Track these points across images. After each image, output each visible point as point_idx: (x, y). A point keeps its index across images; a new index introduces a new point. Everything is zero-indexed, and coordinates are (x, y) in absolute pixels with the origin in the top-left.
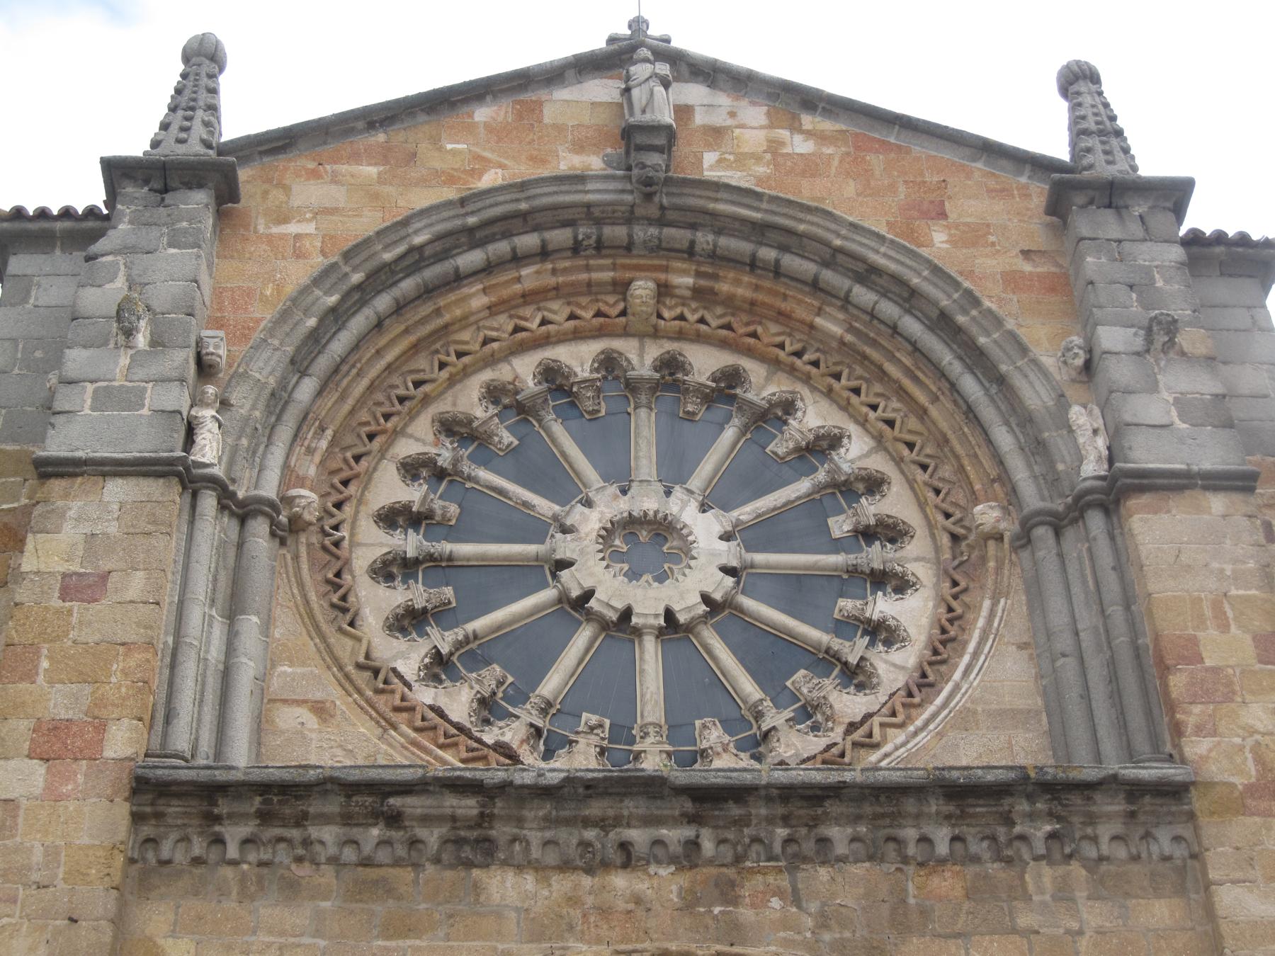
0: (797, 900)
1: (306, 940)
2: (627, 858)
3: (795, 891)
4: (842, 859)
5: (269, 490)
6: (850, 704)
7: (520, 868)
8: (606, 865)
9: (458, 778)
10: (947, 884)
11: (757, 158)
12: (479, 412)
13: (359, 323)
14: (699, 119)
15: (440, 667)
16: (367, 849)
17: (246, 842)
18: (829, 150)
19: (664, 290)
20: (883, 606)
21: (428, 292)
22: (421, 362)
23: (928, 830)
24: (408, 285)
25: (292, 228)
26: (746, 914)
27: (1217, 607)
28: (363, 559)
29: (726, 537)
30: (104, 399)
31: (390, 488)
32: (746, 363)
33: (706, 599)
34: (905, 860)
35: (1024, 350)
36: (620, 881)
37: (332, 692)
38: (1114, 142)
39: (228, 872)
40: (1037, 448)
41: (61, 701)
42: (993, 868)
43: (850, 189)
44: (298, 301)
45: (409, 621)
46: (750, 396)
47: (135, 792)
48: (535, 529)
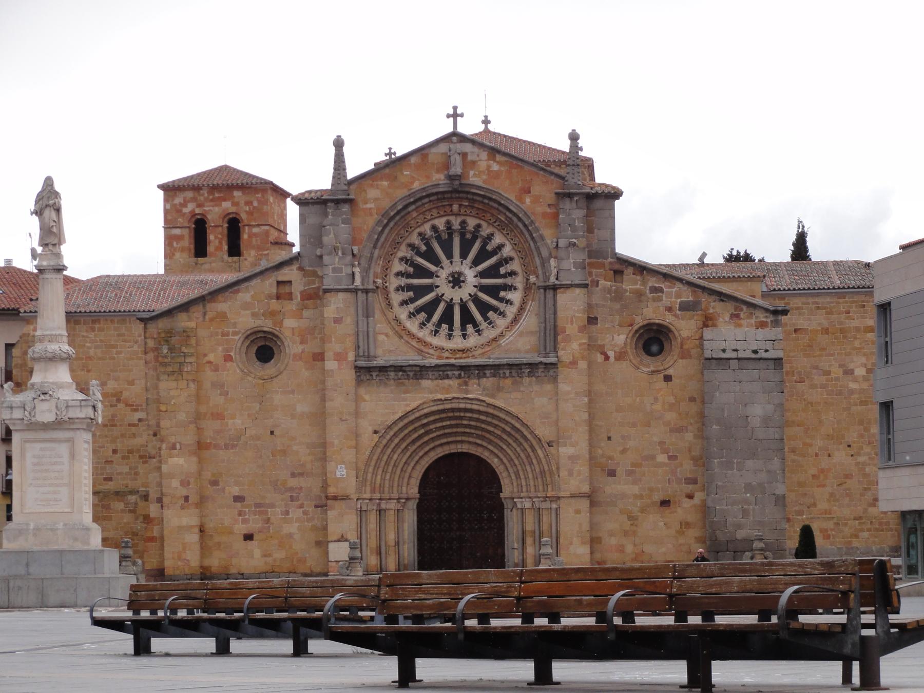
0: (479, 385)
2: (447, 377)
5: (371, 286)
6: (501, 323)
8: (444, 379)
10: (508, 382)
11: (483, 172)
13: (386, 231)
14: (470, 158)
15: (411, 315)
18: (502, 169)
19: (460, 206)
20: (510, 295)
21: (402, 217)
22: (402, 232)
24: (397, 218)
26: (470, 388)
27: (572, 319)
28: (392, 288)
29: (475, 276)
30: (334, 270)
31: (398, 267)
32: (482, 223)
33: (470, 295)
35: (542, 238)
36: (446, 381)
37: (391, 333)
40: (543, 265)
42: (518, 379)
43: (507, 183)
44: (373, 231)
45: (404, 303)
46: (482, 233)
48: (430, 275)
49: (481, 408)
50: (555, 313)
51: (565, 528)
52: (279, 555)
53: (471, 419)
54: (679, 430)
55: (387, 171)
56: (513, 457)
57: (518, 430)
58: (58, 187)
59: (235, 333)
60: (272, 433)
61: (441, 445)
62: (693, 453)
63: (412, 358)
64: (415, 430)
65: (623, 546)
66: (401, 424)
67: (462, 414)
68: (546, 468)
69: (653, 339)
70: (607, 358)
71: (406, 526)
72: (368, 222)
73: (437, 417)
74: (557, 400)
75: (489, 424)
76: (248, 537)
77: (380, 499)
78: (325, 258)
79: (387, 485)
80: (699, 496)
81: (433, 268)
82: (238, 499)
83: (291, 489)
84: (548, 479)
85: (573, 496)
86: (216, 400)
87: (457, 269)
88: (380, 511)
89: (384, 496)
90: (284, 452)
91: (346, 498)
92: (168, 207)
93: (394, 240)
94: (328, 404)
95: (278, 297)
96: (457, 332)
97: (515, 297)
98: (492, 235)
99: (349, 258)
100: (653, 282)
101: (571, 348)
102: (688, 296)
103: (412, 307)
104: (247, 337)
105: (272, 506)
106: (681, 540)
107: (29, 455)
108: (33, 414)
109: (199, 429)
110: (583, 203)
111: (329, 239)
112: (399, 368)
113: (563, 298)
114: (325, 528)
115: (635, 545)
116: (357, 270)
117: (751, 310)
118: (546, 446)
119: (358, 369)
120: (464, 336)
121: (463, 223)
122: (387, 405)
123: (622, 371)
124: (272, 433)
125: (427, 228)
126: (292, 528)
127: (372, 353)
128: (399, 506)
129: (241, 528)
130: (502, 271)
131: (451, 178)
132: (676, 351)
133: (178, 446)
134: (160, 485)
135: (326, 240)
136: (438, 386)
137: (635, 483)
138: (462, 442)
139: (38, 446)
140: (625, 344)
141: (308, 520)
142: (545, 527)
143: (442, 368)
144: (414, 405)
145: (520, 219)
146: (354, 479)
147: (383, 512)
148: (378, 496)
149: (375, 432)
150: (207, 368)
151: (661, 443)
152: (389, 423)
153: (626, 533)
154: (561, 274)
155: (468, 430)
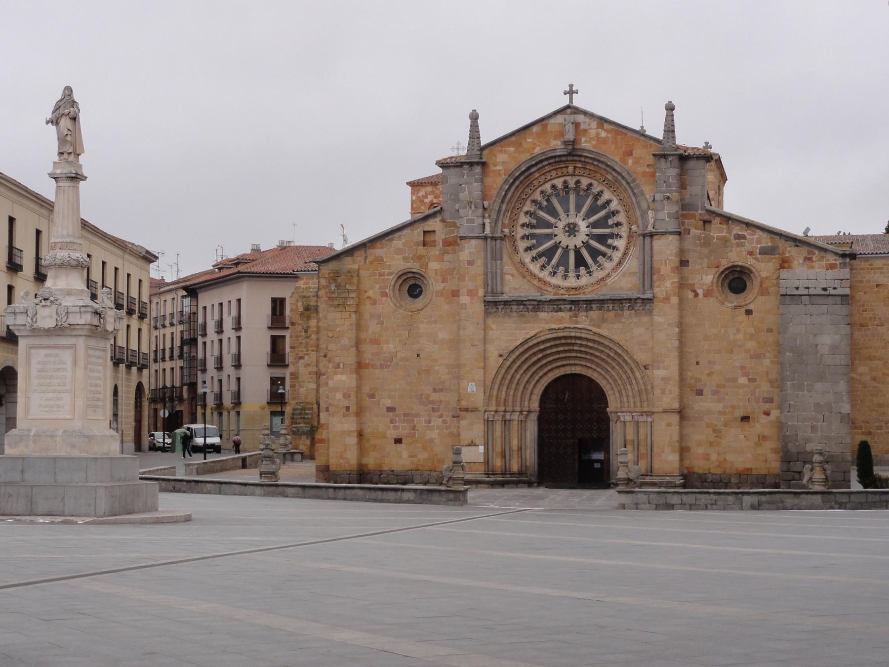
2: (560, 310)
5: (499, 235)
10: (611, 314)
12: (539, 199)
14: (582, 127)
15: (534, 259)
19: (575, 167)
24: (522, 178)
25: (498, 168)
26: (579, 319)
28: (519, 236)
30: (469, 221)
31: (523, 219)
35: (643, 194)
36: (560, 314)
37: (515, 272)
38: (671, 135)
40: (642, 216)
41: (470, 285)
42: (620, 312)
43: (613, 148)
45: (529, 249)
48: (550, 226)
49: (589, 337)
50: (652, 257)
52: (423, 456)
53: (581, 345)
54: (757, 356)
55: (513, 139)
56: (617, 378)
57: (620, 355)
58: (76, 97)
59: (390, 274)
60: (418, 355)
62: (770, 377)
63: (534, 294)
64: (535, 354)
65: (708, 455)
66: (521, 350)
67: (573, 341)
69: (736, 280)
70: (696, 295)
72: (497, 182)
73: (553, 343)
75: (596, 349)
76: (398, 441)
77: (505, 411)
78: (461, 211)
80: (775, 414)
81: (552, 220)
82: (390, 409)
83: (433, 402)
85: (665, 411)
86: (373, 328)
87: (572, 221)
88: (506, 422)
89: (508, 409)
90: (428, 372)
91: (475, 410)
92: (414, 198)
93: (519, 197)
94: (462, 332)
95: (424, 244)
96: (572, 274)
97: (621, 244)
98: (602, 192)
99: (480, 211)
100: (737, 230)
101: (666, 285)
102: (766, 241)
103: (534, 253)
104: (399, 277)
105: (418, 415)
106: (759, 451)
107: (34, 361)
108: (34, 320)
109: (359, 352)
110: (676, 162)
111: (464, 196)
112: (520, 303)
113: (659, 244)
114: (459, 435)
115: (719, 454)
116: (487, 221)
117: (823, 254)
120: (578, 277)
121: (578, 182)
123: (709, 306)
124: (418, 355)
125: (547, 187)
126: (434, 434)
127: (499, 290)
128: (522, 418)
129: (392, 434)
130: (610, 222)
131: (566, 143)
132: (756, 289)
133: (341, 365)
134: (327, 397)
135: (462, 196)
137: (719, 401)
138: (575, 365)
139: (43, 352)
140: (712, 283)
141: (447, 428)
143: (558, 303)
144: (532, 333)
145: (623, 178)
149: (501, 356)
150: (367, 302)
151: (742, 368)
152: (512, 348)
153: (711, 444)
154: (657, 224)
155: (579, 355)
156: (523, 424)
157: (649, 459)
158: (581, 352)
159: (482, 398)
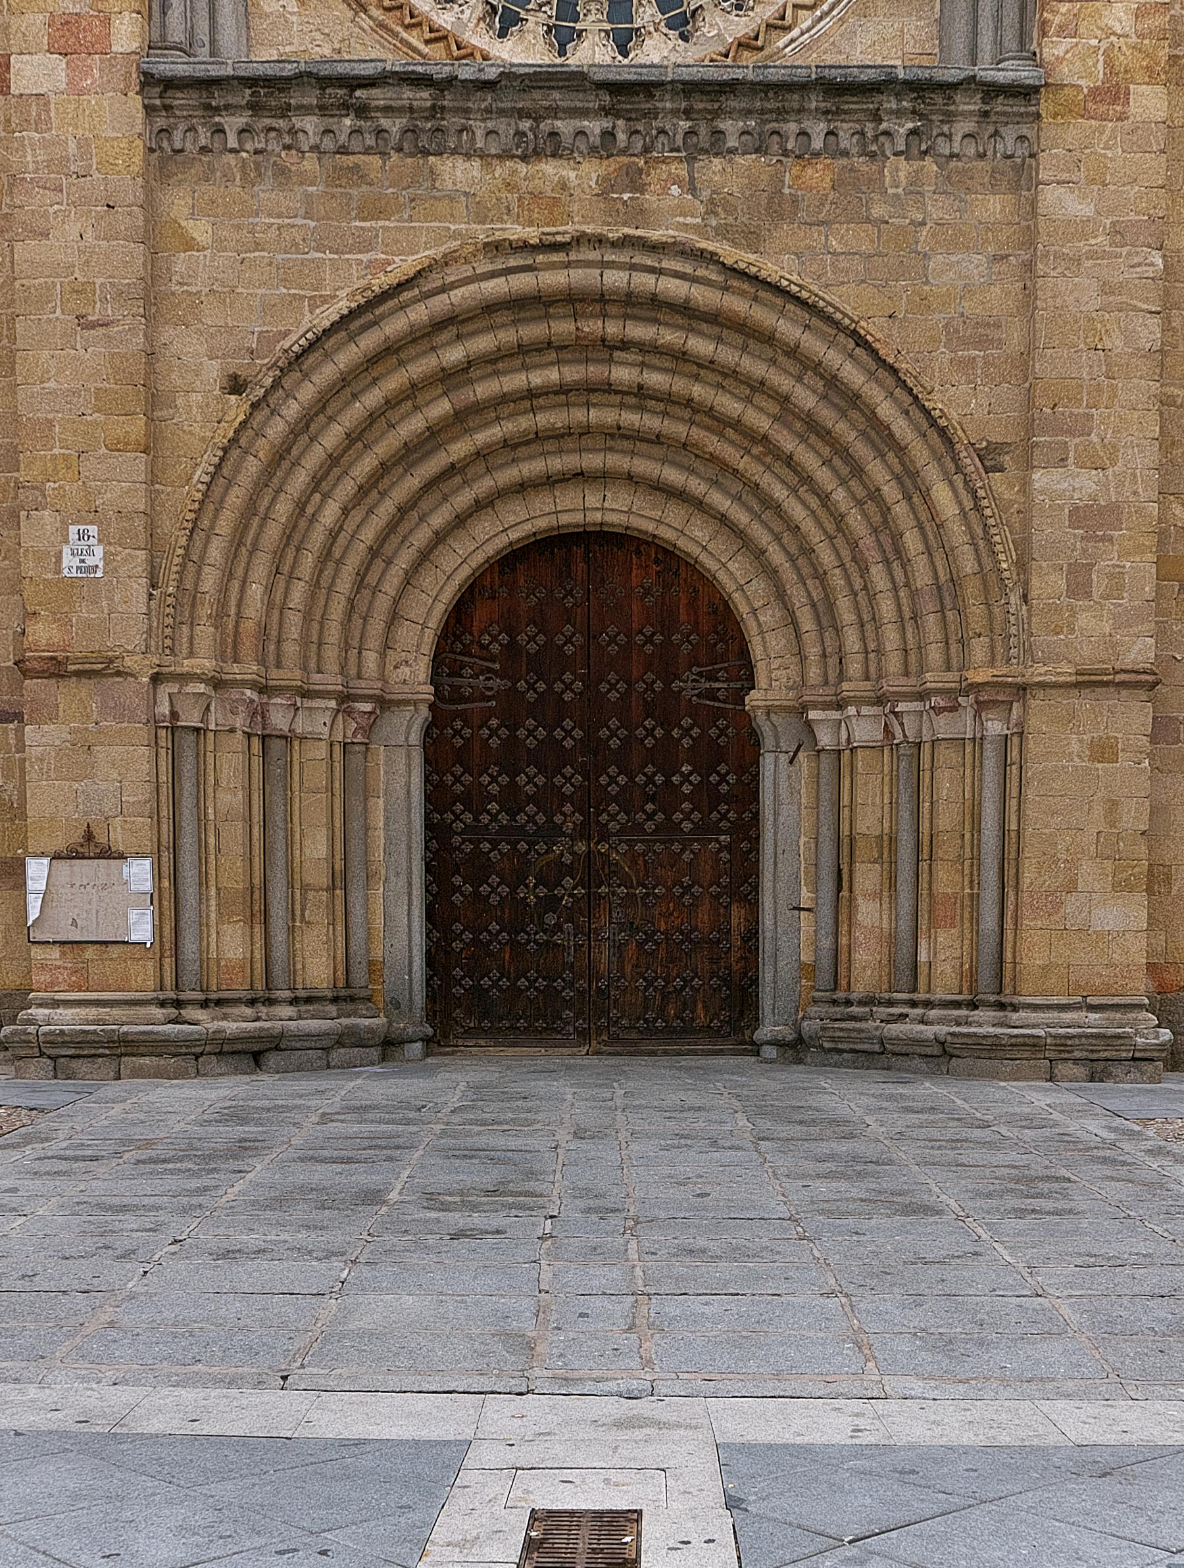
0: (693, 190)
1: (299, 221)
2: (555, 148)
3: (692, 179)
4: (731, 151)
7: (468, 156)
9: (413, 72)
10: (818, 175)
16: (343, 138)
17: (242, 131)
23: (806, 124)
34: (786, 153)
36: (550, 168)
39: (230, 158)
42: (860, 163)
47: (143, 85)
49: (702, 296)
51: (1041, 819)
61: (522, 488)
66: (348, 356)
68: (969, 565)
71: (379, 806)
74: (1029, 266)
79: (293, 631)
84: (976, 611)
88: (268, 743)
89: (277, 676)
91: (102, 670)
112: (341, 90)
118: (970, 462)
119: (159, 89)
122: (279, 258)
136: (510, 186)
138: (603, 477)
142: (947, 819)
144: (405, 265)
146: (139, 587)
147: (276, 746)
148: (249, 669)
149: (236, 385)
152: (294, 341)
155: (631, 419)
156: (356, 760)
157: (989, 922)
158: (641, 395)
159: (140, 605)
